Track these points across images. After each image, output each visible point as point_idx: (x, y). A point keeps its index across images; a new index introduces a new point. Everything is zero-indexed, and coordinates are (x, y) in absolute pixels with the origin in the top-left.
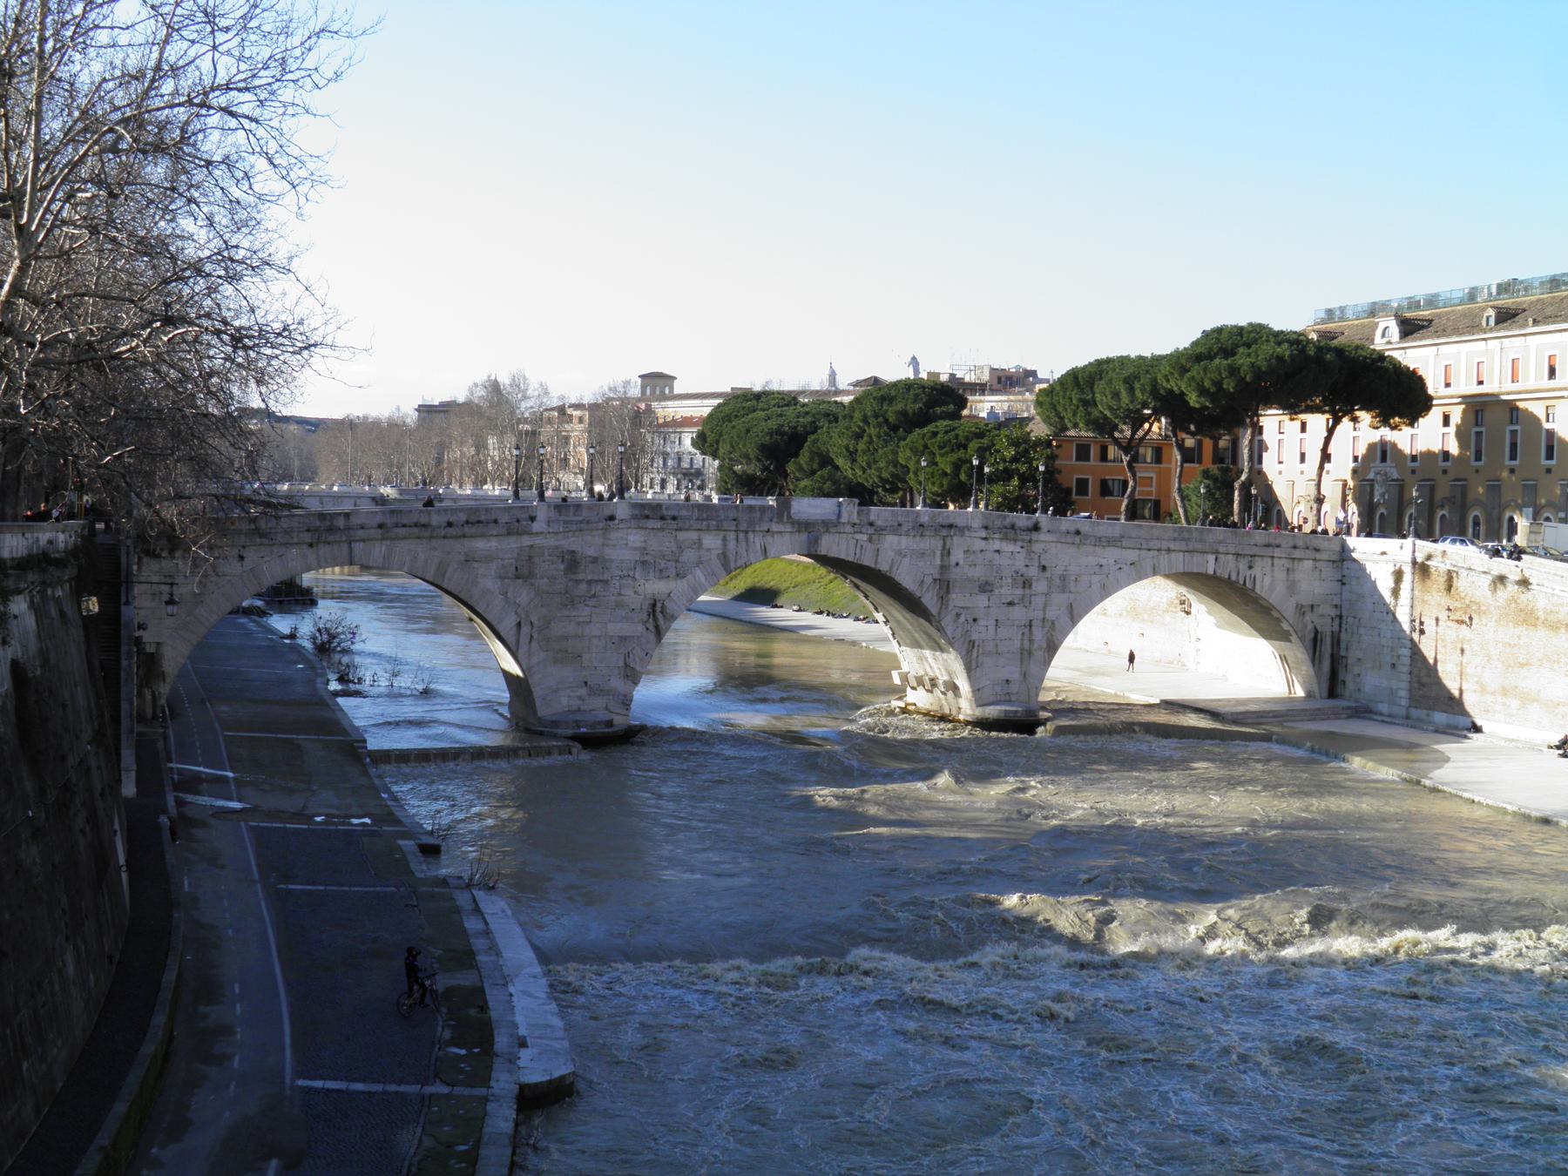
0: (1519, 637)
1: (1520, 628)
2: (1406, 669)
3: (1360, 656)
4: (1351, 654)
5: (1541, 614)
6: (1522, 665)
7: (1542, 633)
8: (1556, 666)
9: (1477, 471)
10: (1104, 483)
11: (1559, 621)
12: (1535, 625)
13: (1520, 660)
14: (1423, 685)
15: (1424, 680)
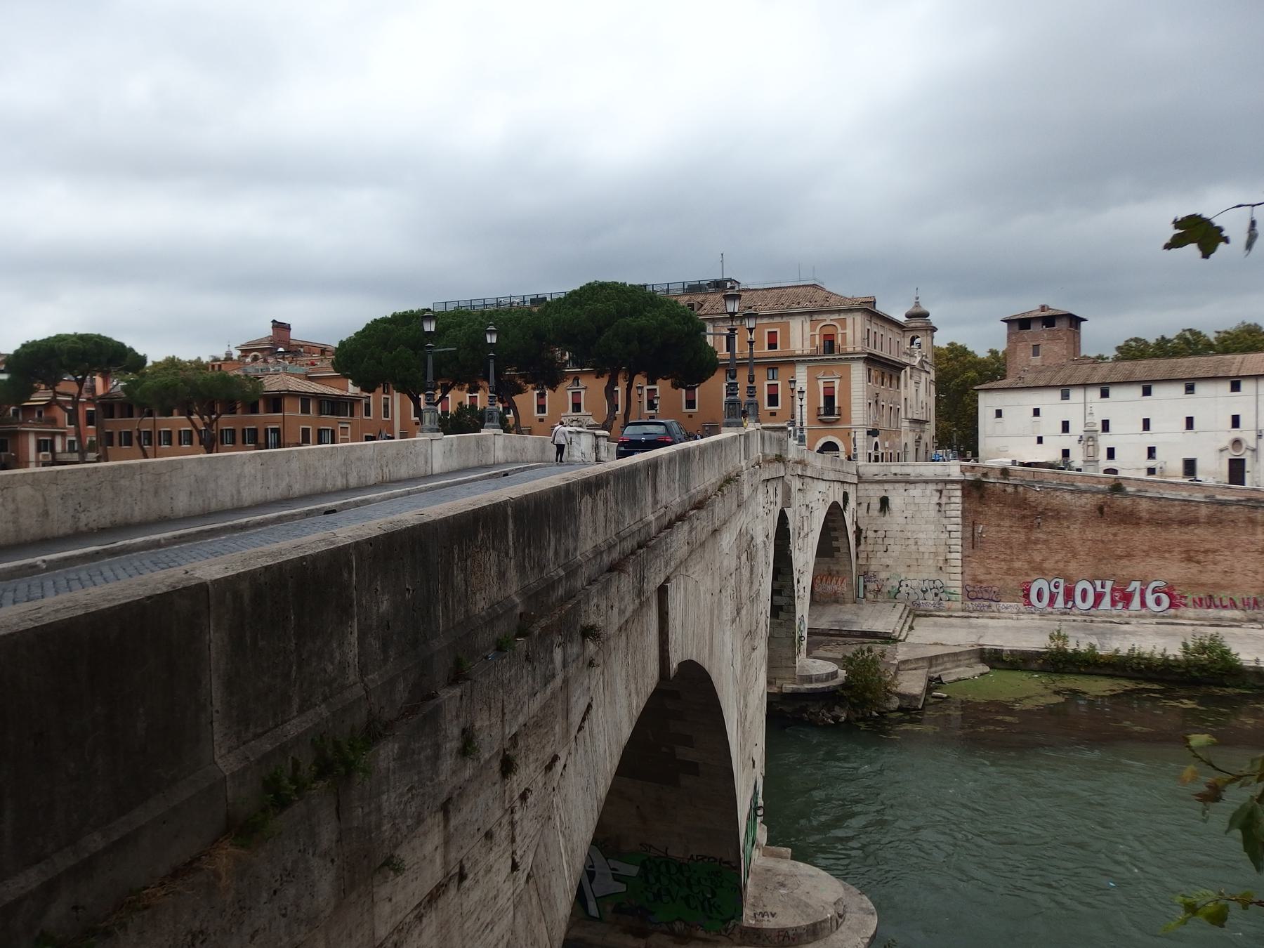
0: (1115, 535)
1: (1116, 528)
2: (959, 570)
3: (889, 562)
4: (873, 562)
5: (1145, 515)
6: (1120, 557)
7: (1146, 530)
8: (1167, 555)
9: (690, 416)
10: (320, 432)
11: (1170, 519)
12: (1137, 524)
13: (1118, 553)
14: (980, 582)
15: (982, 577)
